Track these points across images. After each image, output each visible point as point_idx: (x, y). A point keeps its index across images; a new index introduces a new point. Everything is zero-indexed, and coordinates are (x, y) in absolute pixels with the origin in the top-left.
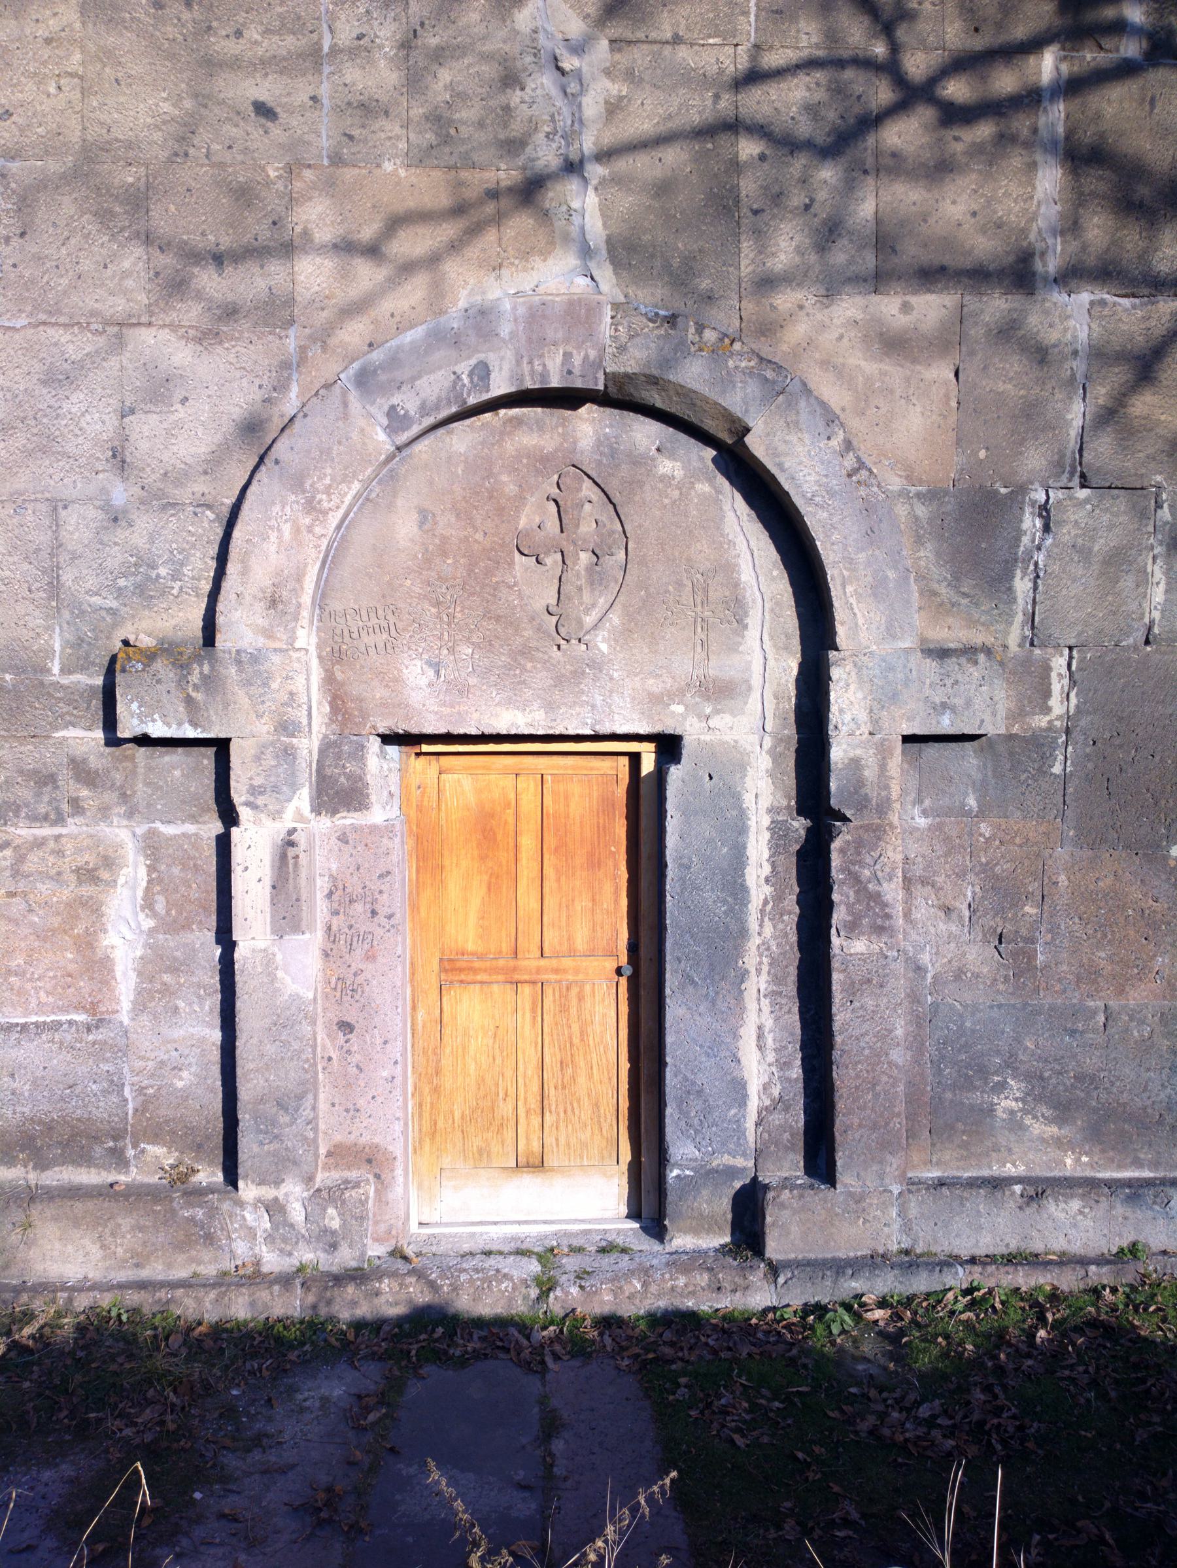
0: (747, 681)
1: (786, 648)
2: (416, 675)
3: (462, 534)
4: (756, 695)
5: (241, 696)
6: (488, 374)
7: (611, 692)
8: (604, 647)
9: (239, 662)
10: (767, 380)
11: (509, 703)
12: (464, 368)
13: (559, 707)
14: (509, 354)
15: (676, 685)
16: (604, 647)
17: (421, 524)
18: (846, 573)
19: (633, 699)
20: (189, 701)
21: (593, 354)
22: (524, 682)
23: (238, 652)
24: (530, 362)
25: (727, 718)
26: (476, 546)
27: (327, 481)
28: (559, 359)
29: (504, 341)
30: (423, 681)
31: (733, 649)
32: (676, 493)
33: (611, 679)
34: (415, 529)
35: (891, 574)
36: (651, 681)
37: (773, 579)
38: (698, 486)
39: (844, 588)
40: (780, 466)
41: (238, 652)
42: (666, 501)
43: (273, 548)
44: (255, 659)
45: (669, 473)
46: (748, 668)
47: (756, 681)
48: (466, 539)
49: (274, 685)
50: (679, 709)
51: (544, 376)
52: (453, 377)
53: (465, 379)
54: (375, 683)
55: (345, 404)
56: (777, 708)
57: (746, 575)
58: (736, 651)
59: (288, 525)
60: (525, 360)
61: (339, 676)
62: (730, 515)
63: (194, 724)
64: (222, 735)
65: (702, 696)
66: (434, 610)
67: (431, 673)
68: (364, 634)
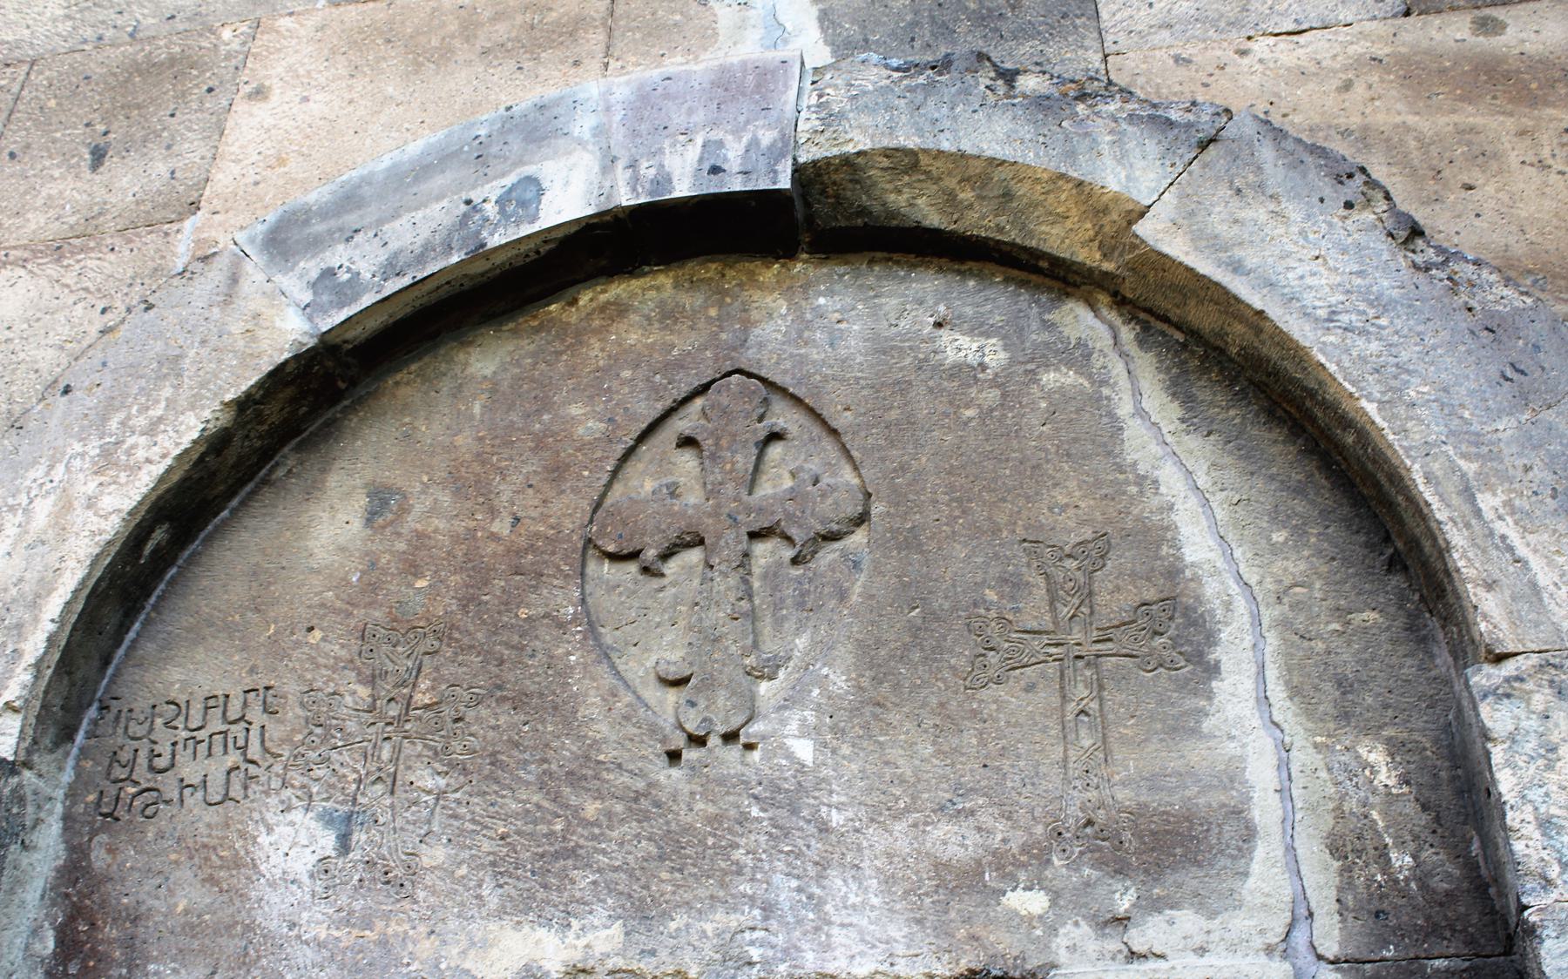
0: (1237, 813)
1: (1345, 716)
3: (460, 526)
6: (540, 192)
7: (822, 865)
8: (804, 750)
10: (1170, 124)
11: (522, 908)
12: (489, 192)
13: (666, 916)
15: (1018, 839)
16: (804, 750)
17: (370, 518)
18: (1471, 468)
19: (888, 881)
21: (767, 137)
22: (572, 853)
24: (633, 165)
25: (1188, 921)
26: (491, 547)
27: (158, 411)
28: (694, 152)
29: (580, 142)
30: (302, 863)
31: (1185, 727)
32: (992, 396)
33: (824, 829)
34: (357, 524)
37: (1275, 550)
38: (1050, 378)
39: (1472, 499)
40: (1237, 267)
42: (970, 413)
45: (973, 359)
46: (1232, 776)
47: (1265, 810)
50: (1030, 902)
51: (663, 180)
52: (463, 208)
53: (491, 209)
54: (185, 873)
55: (234, 280)
56: (1346, 885)
58: (1195, 732)
60: (620, 165)
61: (99, 858)
62: (1134, 431)
65: (1098, 864)
66: (364, 692)
67: (327, 841)
68: (183, 757)
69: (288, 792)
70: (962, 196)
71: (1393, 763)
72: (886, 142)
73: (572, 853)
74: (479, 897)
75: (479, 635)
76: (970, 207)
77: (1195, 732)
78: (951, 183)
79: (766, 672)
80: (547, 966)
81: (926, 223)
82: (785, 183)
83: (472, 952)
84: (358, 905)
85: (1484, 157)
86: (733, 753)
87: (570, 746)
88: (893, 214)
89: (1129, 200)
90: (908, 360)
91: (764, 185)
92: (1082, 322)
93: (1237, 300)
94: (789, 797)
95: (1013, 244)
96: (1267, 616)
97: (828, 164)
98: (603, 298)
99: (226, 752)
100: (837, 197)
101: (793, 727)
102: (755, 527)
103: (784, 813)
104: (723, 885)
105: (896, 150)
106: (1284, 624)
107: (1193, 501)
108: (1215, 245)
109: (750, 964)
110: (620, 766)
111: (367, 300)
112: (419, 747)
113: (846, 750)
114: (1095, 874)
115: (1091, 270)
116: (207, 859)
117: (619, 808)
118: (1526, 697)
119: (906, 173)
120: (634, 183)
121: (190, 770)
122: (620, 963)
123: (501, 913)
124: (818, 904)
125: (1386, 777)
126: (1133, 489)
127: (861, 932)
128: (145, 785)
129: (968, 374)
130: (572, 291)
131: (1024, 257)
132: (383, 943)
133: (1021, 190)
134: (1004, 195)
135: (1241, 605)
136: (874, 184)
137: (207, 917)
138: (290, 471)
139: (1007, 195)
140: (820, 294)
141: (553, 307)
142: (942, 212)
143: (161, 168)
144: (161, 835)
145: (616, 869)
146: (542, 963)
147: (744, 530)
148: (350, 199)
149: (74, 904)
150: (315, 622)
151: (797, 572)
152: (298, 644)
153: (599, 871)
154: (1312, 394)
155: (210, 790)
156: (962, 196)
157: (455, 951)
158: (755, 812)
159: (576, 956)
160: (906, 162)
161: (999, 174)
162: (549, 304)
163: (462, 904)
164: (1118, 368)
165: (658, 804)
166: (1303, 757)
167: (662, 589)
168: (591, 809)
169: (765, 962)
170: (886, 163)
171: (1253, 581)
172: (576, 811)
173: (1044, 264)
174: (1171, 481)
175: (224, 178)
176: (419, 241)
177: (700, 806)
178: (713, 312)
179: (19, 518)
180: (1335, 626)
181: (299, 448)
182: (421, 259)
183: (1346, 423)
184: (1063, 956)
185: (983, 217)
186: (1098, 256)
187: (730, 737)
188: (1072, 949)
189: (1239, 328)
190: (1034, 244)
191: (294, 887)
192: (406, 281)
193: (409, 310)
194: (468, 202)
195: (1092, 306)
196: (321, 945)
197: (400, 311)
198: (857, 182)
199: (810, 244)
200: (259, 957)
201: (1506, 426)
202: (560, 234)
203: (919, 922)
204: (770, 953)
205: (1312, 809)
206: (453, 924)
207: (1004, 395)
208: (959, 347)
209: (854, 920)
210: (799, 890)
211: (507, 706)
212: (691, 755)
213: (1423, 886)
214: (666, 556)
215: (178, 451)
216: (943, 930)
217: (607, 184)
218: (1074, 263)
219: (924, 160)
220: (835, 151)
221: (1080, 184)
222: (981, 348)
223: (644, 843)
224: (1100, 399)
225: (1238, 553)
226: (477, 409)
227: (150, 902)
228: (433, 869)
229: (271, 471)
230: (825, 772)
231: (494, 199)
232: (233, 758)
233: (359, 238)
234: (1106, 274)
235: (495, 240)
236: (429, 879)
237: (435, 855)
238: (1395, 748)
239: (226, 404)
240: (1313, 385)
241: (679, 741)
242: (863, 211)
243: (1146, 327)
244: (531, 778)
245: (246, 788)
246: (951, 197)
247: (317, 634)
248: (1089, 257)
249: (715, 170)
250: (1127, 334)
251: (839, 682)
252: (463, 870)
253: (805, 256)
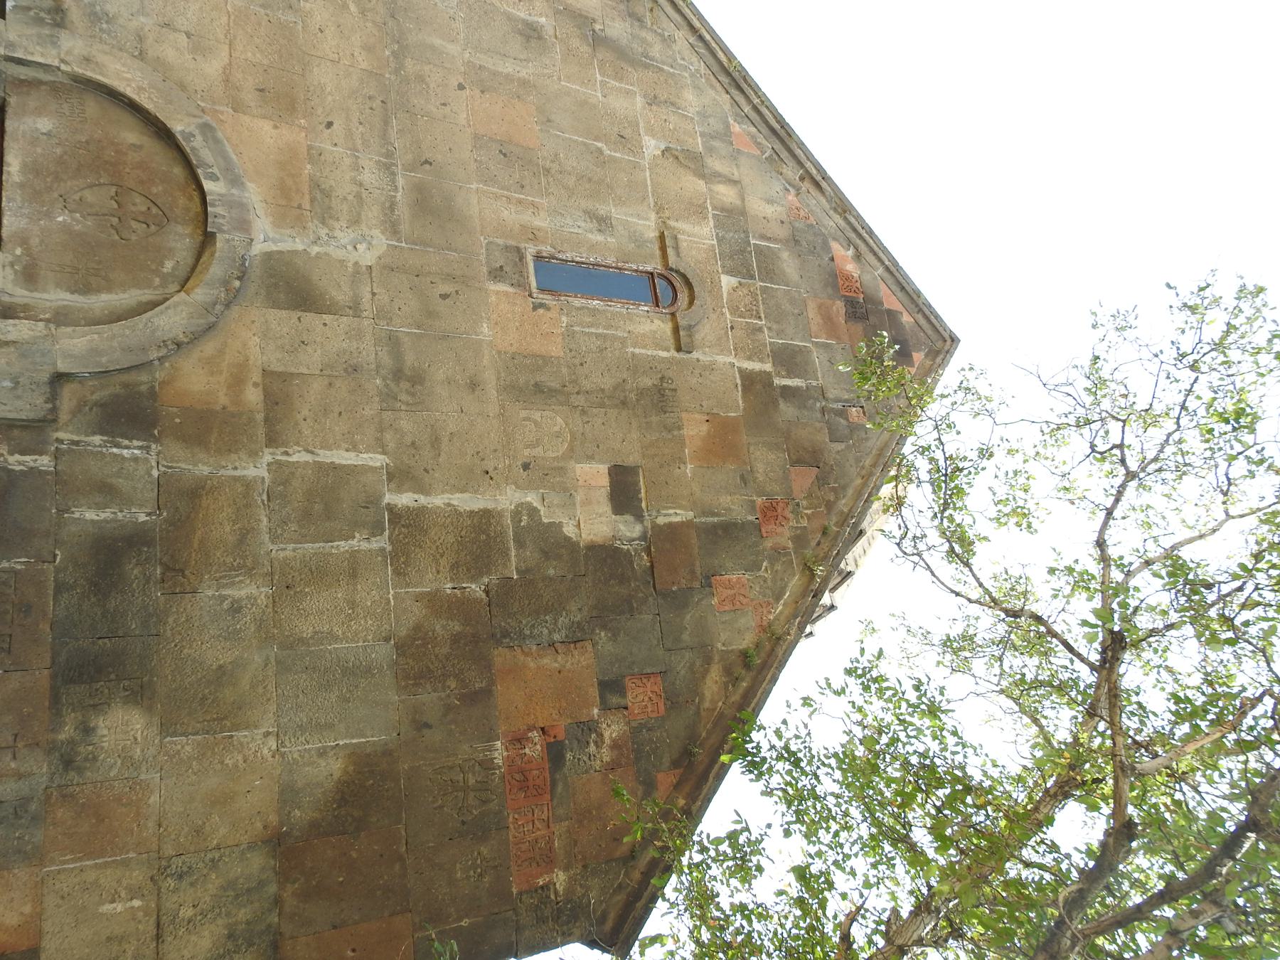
0: (36, 290)
8: (60, 219)
9: (52, 36)
14: (223, 191)
20: (29, 9)
30: (39, 126)
35: (104, 360)
36: (37, 240)
40: (167, 308)
46: (45, 291)
49: (38, 48)
57: (104, 297)
61: (43, 87)
62: (139, 292)
63: (14, 7)
85: (212, 374)
86: (61, 206)
94: (49, 215)
129: (162, 264)
143: (252, 104)
148: (217, 141)
160: (212, 255)
166: (48, 304)
174: (126, 296)
175: (246, 119)
237: (39, 150)
251: (77, 228)
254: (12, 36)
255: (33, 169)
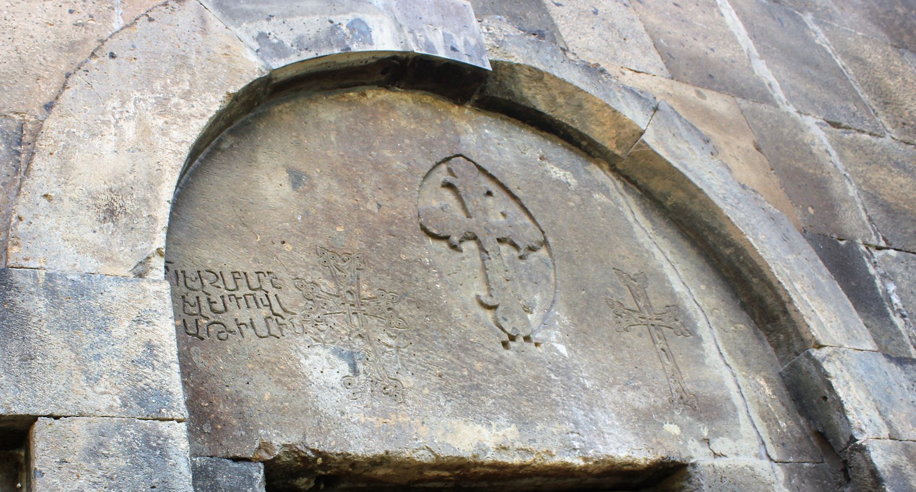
2: (322, 367)
3: (351, 202)
4: (742, 416)
5: (56, 344)
7: (590, 404)
8: (562, 349)
22: (477, 387)
23: (50, 277)
26: (371, 217)
30: (334, 378)
33: (584, 388)
34: (287, 188)
36: (630, 394)
40: (686, 167)
41: (50, 277)
43: (109, 147)
44: (79, 291)
46: (721, 385)
48: (356, 208)
49: (120, 330)
52: (330, 25)
57: (678, 287)
59: (132, 124)
62: (636, 228)
64: (19, 410)
67: (344, 367)
68: (231, 305)
69: (308, 336)
70: (558, 100)
71: (770, 387)
72: (529, 63)
73: (477, 387)
74: (439, 406)
75: (385, 264)
76: (561, 106)
77: (703, 364)
78: (555, 92)
79: (528, 309)
80: (488, 444)
81: (538, 108)
82: (489, 67)
83: (448, 435)
84: (376, 404)
87: (455, 334)
88: (523, 99)
89: (636, 125)
90: (536, 172)
91: (479, 64)
92: (600, 174)
93: (689, 181)
94: (564, 370)
95: (576, 130)
96: (711, 319)
97: (502, 65)
98: (379, 97)
99: (258, 307)
100: (500, 82)
101: (553, 338)
102: (500, 236)
103: (565, 379)
104: (553, 411)
105: (535, 68)
106: (716, 324)
107: (669, 266)
108: (673, 154)
109: (575, 449)
110: (483, 345)
111: (293, 59)
112: (376, 321)
113: (579, 352)
114: (691, 420)
115: (609, 152)
116: (273, 369)
117: (491, 367)
118: (834, 362)
119: (535, 81)
120: (417, 41)
121: (244, 315)
122: (522, 446)
123: (454, 415)
124: (596, 424)
125: (768, 391)
126: (647, 255)
127: (617, 437)
128: (213, 320)
130: (361, 88)
131: (576, 137)
132: (399, 427)
133: (587, 106)
134: (579, 106)
135: (701, 315)
136: (519, 82)
137: (287, 404)
138: (232, 146)
139: (580, 106)
140: (485, 128)
141: (351, 94)
142: (547, 105)
144: (235, 351)
145: (501, 398)
146: (485, 442)
147: (495, 237)
149: (193, 389)
150: (284, 239)
151: (522, 263)
152: (279, 251)
153: (494, 398)
154: (712, 229)
155: (257, 328)
156: (558, 100)
157: (440, 434)
158: (553, 377)
159: (500, 440)
160: (538, 76)
161: (578, 95)
162: (349, 92)
163: (433, 409)
164: (621, 200)
165: (508, 367)
167: (463, 258)
168: (478, 366)
169: (581, 449)
170: (528, 73)
171: (701, 304)
172: (471, 366)
173: (584, 143)
176: (312, 33)
177: (527, 370)
178: (438, 122)
179: (113, 130)
180: (733, 328)
181: (232, 132)
182: (317, 43)
183: (729, 244)
184: (693, 454)
185: (565, 113)
186: (614, 146)
187: (527, 339)
188: (695, 450)
189: (681, 194)
190: (586, 132)
191: (335, 392)
192: (312, 55)
193: (304, 71)
194: (331, 22)
195: (601, 168)
196: (364, 425)
197: (302, 71)
198: (512, 78)
199: (477, 101)
200: (329, 430)
201: (790, 257)
202: (380, 56)
203: (637, 434)
204: (583, 445)
205: (751, 401)
206: (433, 419)
207: (582, 199)
208: (557, 173)
209: (612, 431)
210: (585, 416)
211: (414, 306)
212: (512, 344)
213: (792, 435)
214: (461, 242)
215: (211, 115)
216: (646, 437)
217: (403, 38)
218: (602, 146)
219: (546, 78)
220: (505, 59)
221: (615, 111)
222: (564, 175)
223: (509, 386)
224: (619, 211)
225: (692, 291)
226: (333, 139)
227: (245, 392)
228: (411, 388)
229: (221, 141)
230: (575, 361)
231: (345, 25)
232: (265, 311)
233: (273, 20)
234: (615, 155)
235: (355, 48)
236: (410, 394)
237: (408, 380)
238: (767, 380)
239: (229, 94)
240: (716, 225)
241: (506, 338)
242: (511, 93)
243: (625, 185)
244: (442, 346)
245: (281, 330)
246: (553, 100)
247: (288, 247)
248: (610, 145)
249: (453, 49)
250: (620, 185)
251: (566, 320)
252: (426, 391)
253: (469, 106)
254: (105, 398)
255: (468, 396)
